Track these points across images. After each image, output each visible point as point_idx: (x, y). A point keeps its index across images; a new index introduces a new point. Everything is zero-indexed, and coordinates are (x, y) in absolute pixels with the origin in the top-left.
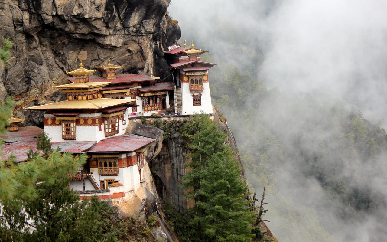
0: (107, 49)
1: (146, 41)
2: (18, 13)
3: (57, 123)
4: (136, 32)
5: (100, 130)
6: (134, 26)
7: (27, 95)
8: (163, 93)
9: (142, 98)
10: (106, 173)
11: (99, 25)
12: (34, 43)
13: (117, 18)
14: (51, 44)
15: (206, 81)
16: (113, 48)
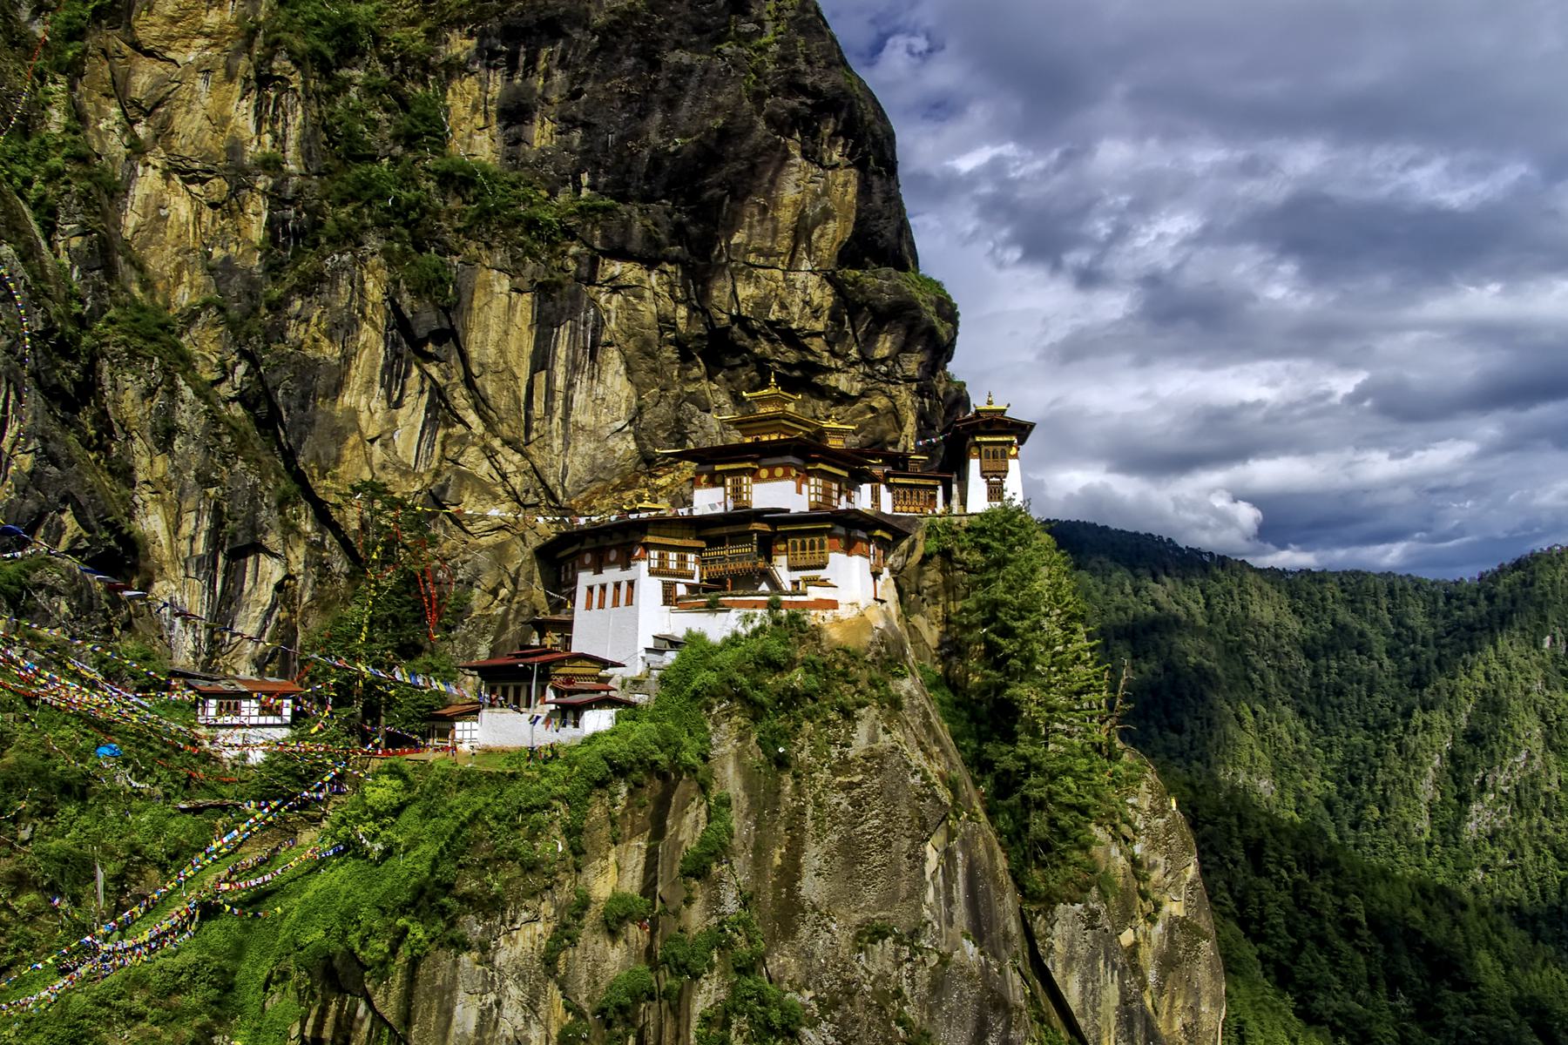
0: (831, 398)
1: (904, 395)
2: (667, 305)
3: (718, 479)
4: (887, 374)
5: (799, 491)
6: (883, 361)
7: (678, 469)
8: (931, 483)
9: (890, 487)
10: (803, 563)
11: (817, 344)
12: (696, 370)
13: (850, 340)
14: (729, 380)
15: (1015, 456)
16: (843, 399)
